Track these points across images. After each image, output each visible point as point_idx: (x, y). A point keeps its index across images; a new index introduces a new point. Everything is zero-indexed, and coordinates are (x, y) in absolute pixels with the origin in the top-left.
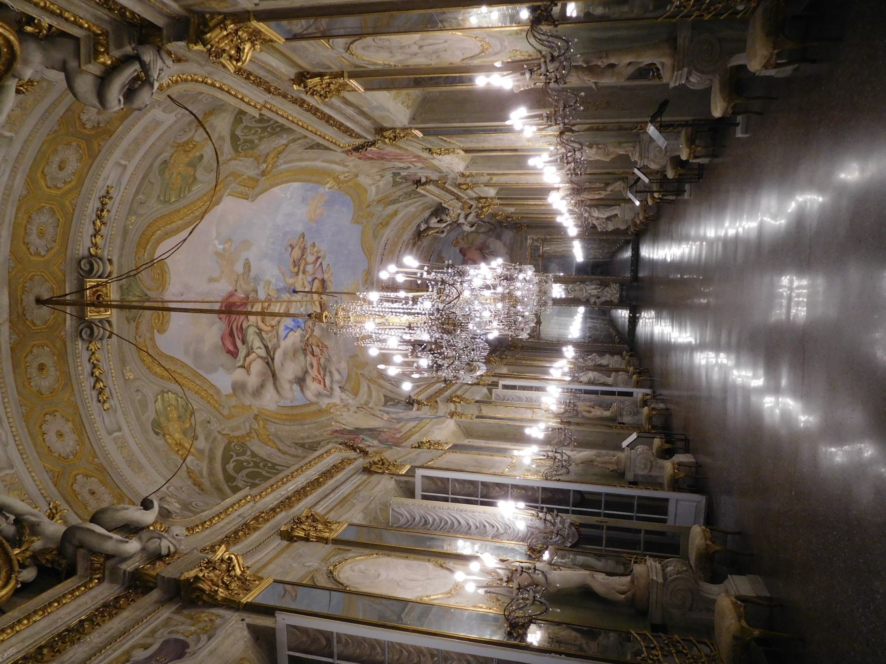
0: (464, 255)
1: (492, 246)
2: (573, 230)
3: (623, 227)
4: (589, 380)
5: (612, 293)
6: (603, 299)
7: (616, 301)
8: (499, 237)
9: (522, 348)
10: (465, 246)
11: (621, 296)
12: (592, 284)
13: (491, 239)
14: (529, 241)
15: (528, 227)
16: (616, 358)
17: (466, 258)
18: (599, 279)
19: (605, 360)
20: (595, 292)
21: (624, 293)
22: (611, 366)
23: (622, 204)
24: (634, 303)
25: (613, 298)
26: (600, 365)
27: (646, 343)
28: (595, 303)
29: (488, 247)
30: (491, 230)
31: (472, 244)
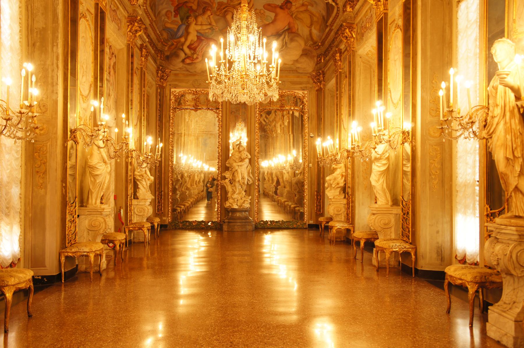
0: (281, 7)
1: (293, 44)
2: (325, 144)
3: (330, 210)
4: (92, 168)
5: (238, 199)
6: (229, 188)
7: (227, 205)
8: (305, 53)
9: (162, 88)
10: (293, 8)
11: (234, 211)
12: (249, 173)
13: (302, 43)
14: (301, 92)
15: (319, 90)
16: (149, 211)
17: (278, 10)
18: (254, 183)
19: (146, 195)
20: (239, 178)
21: (238, 214)
22: (134, 202)
23: (398, 210)
24: (225, 228)
25: (231, 201)
26: (136, 187)
27: (174, 250)
28: (224, 178)
29: (292, 40)
30: (315, 43)
31: (296, 18)
